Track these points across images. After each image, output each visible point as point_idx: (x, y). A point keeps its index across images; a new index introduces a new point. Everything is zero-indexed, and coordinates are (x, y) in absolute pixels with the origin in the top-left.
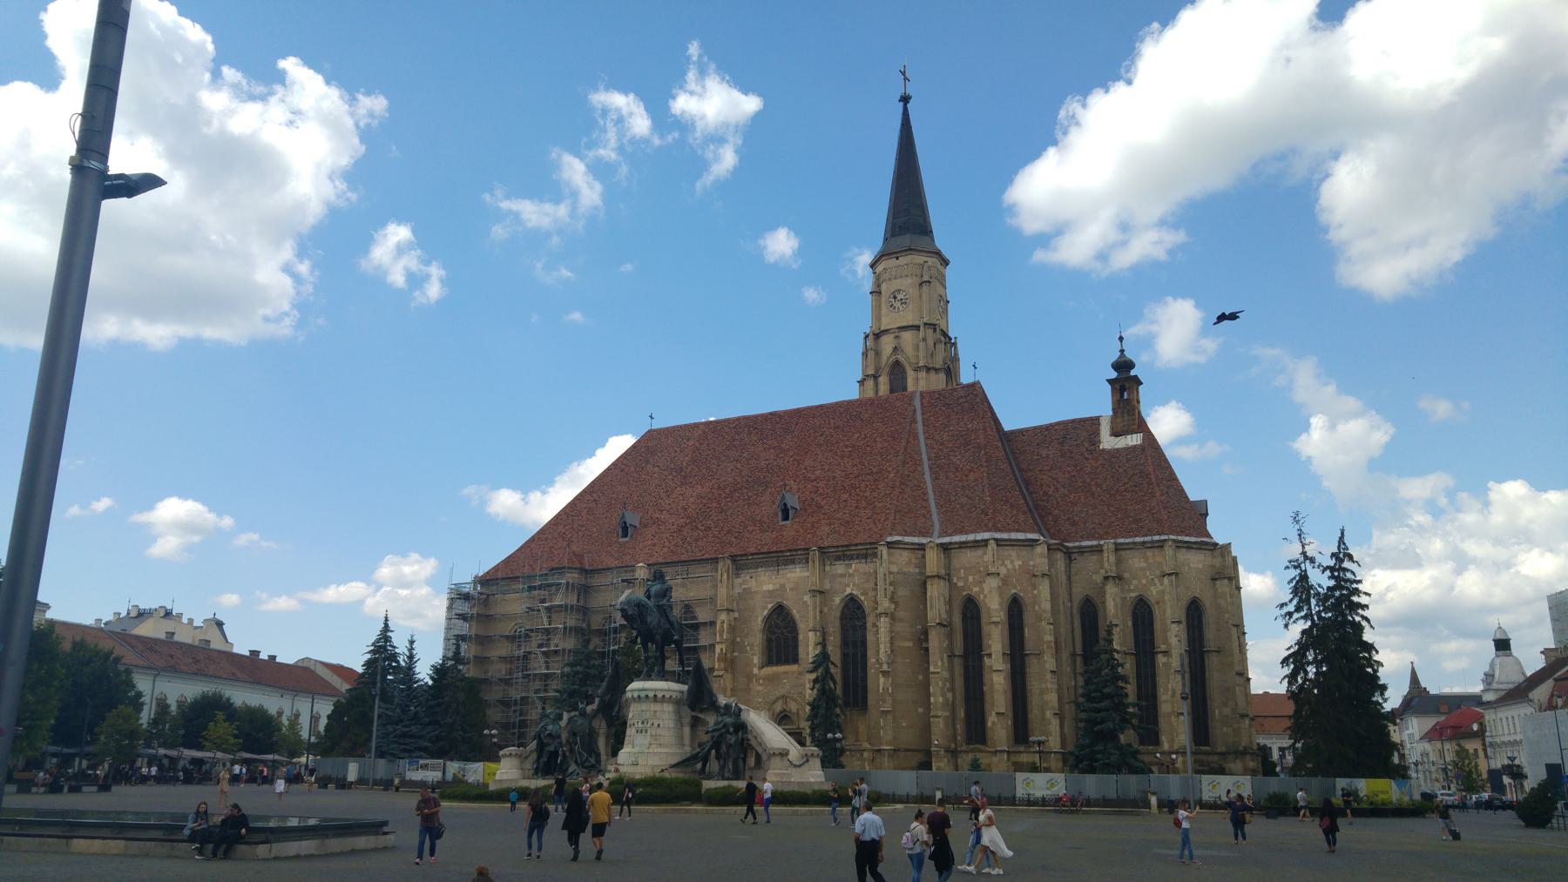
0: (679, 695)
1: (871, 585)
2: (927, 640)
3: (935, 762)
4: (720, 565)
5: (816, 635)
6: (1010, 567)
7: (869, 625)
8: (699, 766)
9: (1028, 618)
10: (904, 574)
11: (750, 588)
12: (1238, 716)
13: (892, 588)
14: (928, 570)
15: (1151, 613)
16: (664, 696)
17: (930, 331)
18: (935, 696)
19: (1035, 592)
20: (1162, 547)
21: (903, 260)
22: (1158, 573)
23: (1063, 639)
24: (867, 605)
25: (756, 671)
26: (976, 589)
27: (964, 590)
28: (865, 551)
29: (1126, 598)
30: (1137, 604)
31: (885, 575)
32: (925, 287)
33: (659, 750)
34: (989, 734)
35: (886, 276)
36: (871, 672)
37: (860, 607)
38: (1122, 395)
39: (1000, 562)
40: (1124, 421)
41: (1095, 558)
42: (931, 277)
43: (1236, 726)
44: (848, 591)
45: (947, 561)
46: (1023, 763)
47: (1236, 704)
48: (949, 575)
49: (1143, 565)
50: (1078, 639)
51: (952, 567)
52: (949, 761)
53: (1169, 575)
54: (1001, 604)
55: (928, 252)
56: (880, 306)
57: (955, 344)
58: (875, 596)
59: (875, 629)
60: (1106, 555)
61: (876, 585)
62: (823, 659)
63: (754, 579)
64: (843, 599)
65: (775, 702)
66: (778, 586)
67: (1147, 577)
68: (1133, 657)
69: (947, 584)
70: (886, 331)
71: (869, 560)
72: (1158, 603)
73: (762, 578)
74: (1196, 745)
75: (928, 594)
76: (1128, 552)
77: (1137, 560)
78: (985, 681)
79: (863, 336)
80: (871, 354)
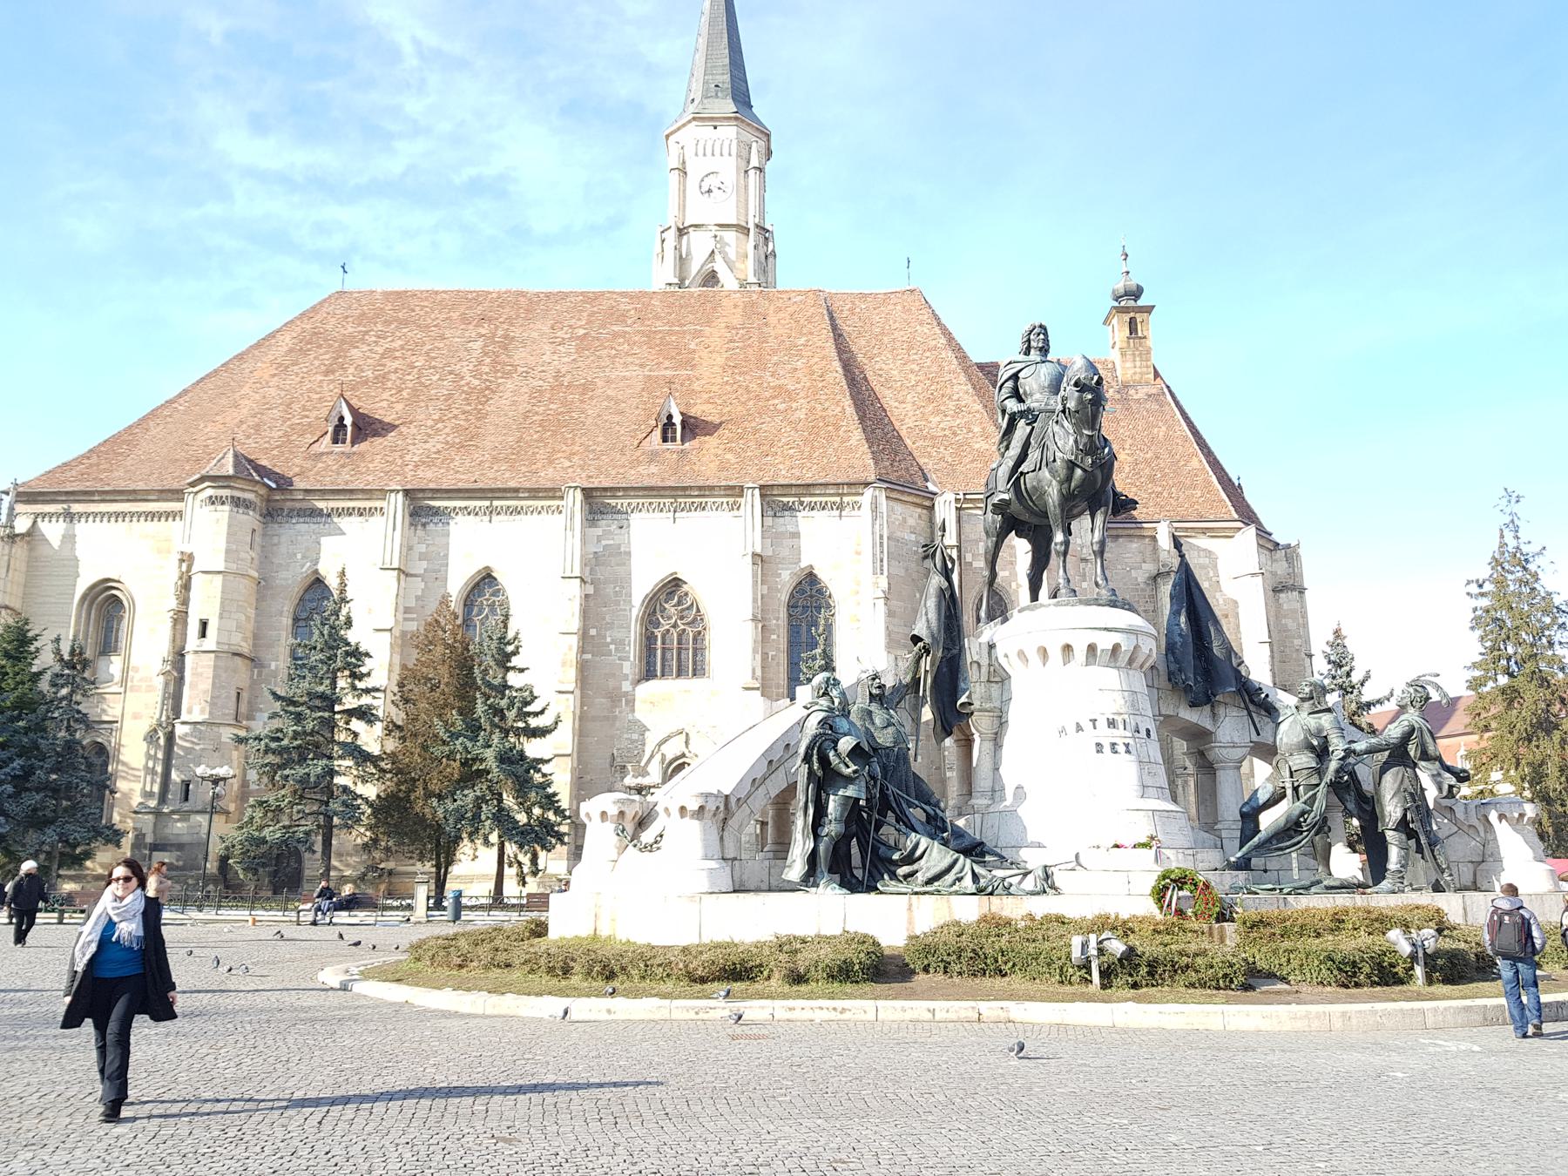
5: (756, 627)
26: (1006, 573)
31: (881, 537)
51: (962, 537)
63: (623, 530)
71: (844, 513)
72: (1227, 616)
77: (1196, 553)
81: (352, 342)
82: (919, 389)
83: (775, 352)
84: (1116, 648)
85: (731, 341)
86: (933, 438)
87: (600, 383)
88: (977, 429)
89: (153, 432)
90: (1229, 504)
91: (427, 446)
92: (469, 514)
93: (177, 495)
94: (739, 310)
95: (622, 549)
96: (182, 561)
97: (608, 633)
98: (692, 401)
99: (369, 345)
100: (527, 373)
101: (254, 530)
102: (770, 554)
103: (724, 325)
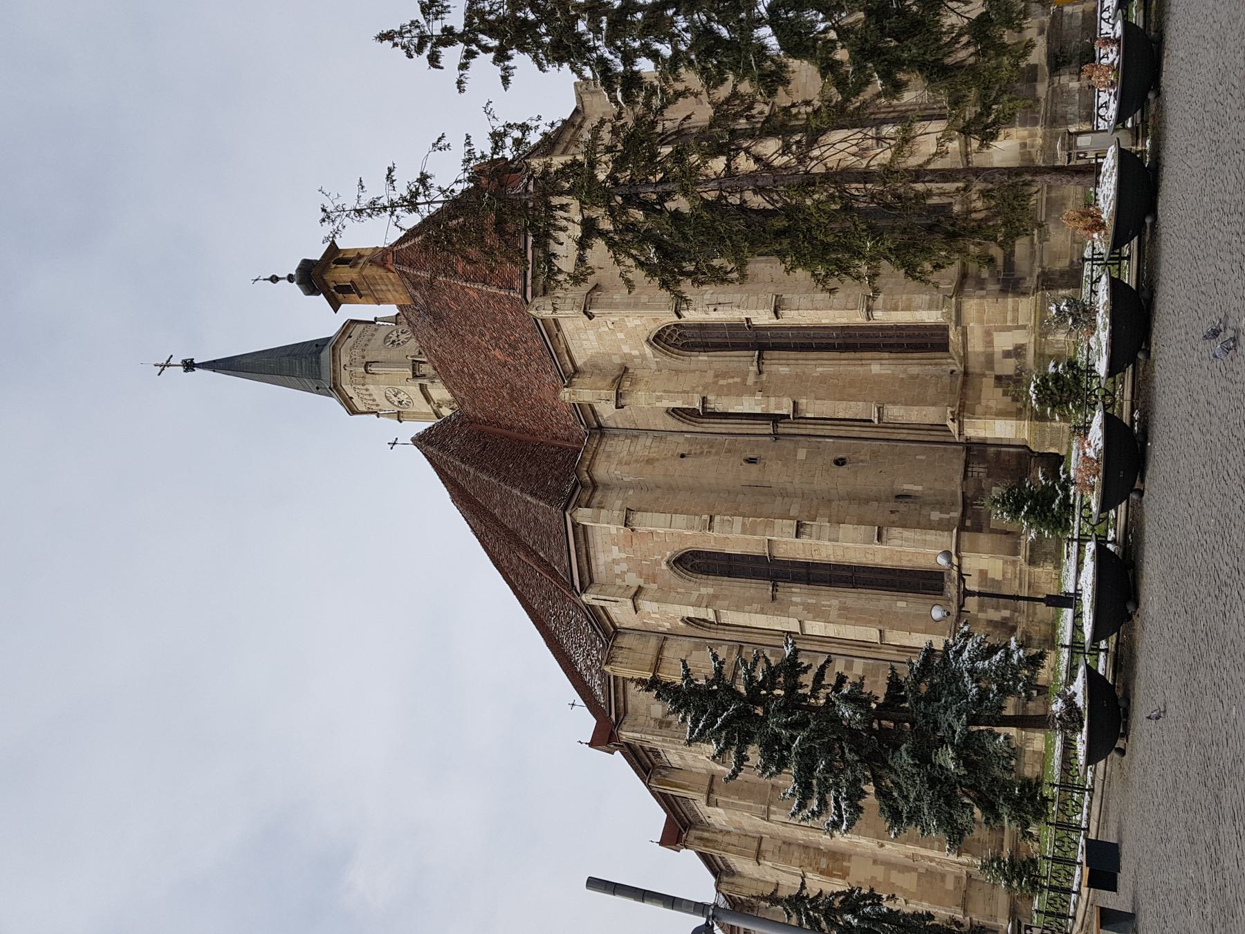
5: (775, 813)
6: (624, 567)
40: (389, 290)
68: (767, 354)
76: (574, 353)
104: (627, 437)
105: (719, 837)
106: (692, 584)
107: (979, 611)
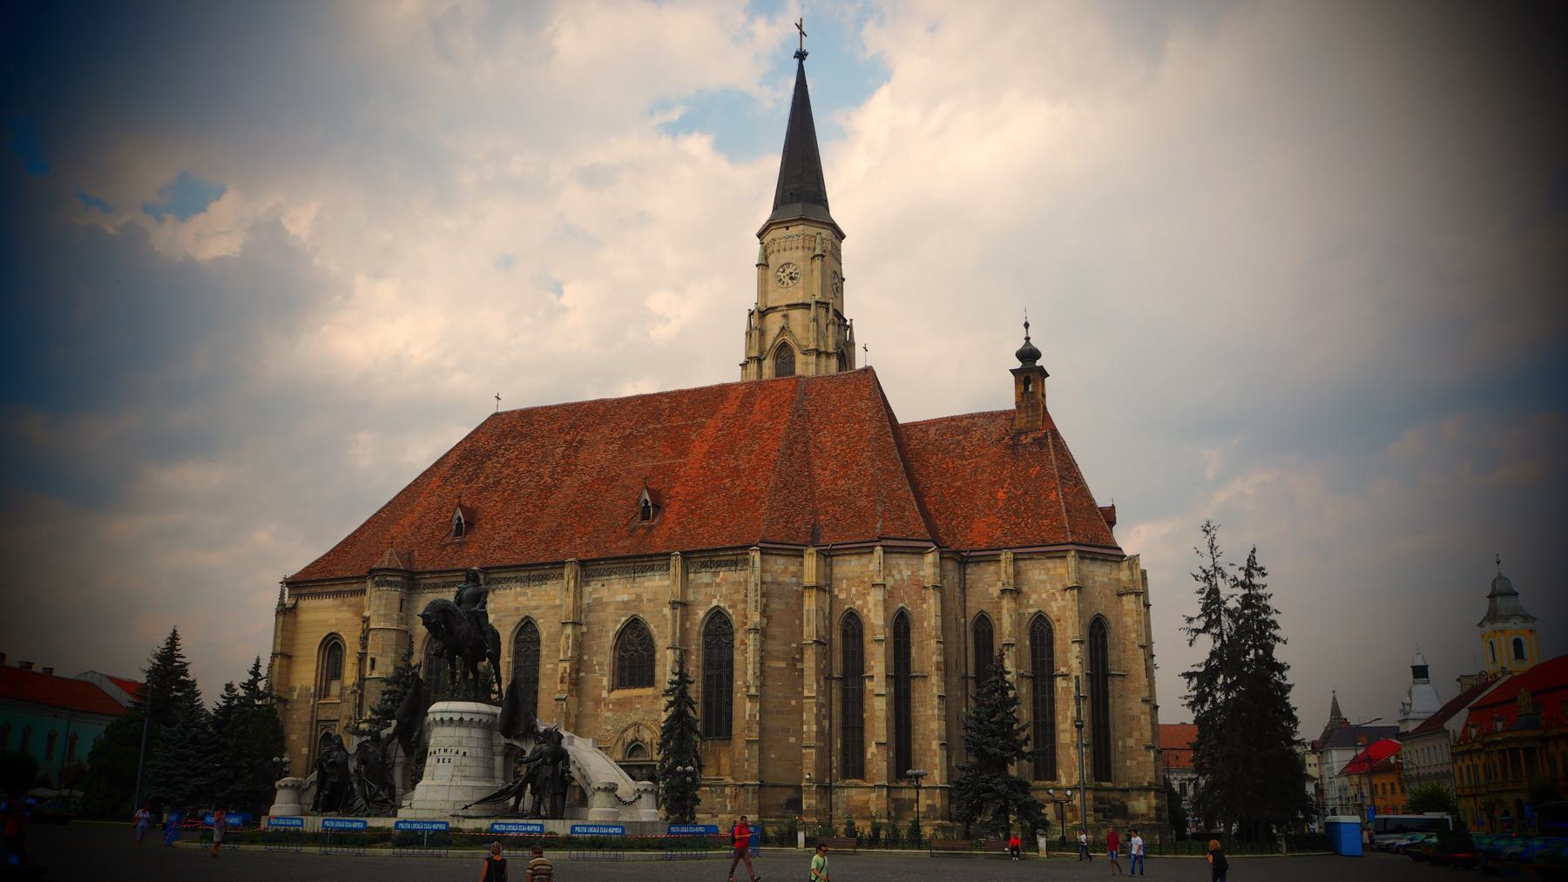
0: (491, 719)
1: (743, 596)
2: (801, 660)
3: (806, 798)
4: (567, 571)
5: (675, 653)
6: (898, 577)
7: (737, 643)
8: (512, 801)
9: (915, 636)
10: (779, 584)
11: (602, 598)
12: (1143, 748)
13: (764, 600)
14: (806, 580)
15: (1051, 631)
16: (472, 719)
17: (823, 311)
18: (809, 724)
19: (925, 606)
20: (1065, 557)
21: (794, 230)
22: (1060, 586)
23: (954, 659)
24: (735, 619)
25: (605, 694)
26: (859, 603)
27: (846, 604)
28: (734, 558)
29: (1024, 614)
30: (1036, 621)
31: (756, 585)
32: (818, 262)
33: (464, 783)
34: (868, 767)
35: (776, 247)
36: (738, 696)
37: (727, 622)
38: (1026, 388)
39: (887, 572)
41: (992, 568)
42: (824, 251)
43: (1141, 759)
44: (715, 603)
45: (828, 570)
46: (905, 799)
47: (1142, 735)
48: (830, 585)
49: (1044, 577)
50: (971, 660)
51: (833, 576)
52: (822, 798)
53: (1072, 588)
54: (885, 619)
55: (822, 223)
56: (766, 281)
57: (850, 327)
58: (745, 609)
59: (743, 647)
60: (1003, 565)
61: (746, 596)
62: (683, 680)
64: (708, 613)
65: (626, 730)
66: (634, 597)
67: (1047, 592)
69: (828, 596)
70: (773, 309)
71: (738, 568)
72: (1059, 620)
73: (616, 587)
74: (1096, 781)
75: (806, 608)
76: (1028, 562)
78: (866, 707)
79: (747, 313)
80: (756, 334)
81: (488, 455)
82: (840, 458)
83: (746, 436)
84: (451, 719)
85: (720, 430)
86: (835, 498)
87: (623, 474)
88: (865, 490)
89: (366, 534)
90: (1068, 529)
91: (506, 534)
92: (518, 581)
93: (361, 579)
94: (738, 400)
95: (604, 601)
96: (363, 622)
97: (594, 658)
98: (674, 485)
99: (498, 457)
100: (582, 470)
101: (402, 601)
102: (693, 599)
103: (721, 416)
104: (960, 579)
105: (579, 590)
106: (890, 621)
107: (892, 799)
